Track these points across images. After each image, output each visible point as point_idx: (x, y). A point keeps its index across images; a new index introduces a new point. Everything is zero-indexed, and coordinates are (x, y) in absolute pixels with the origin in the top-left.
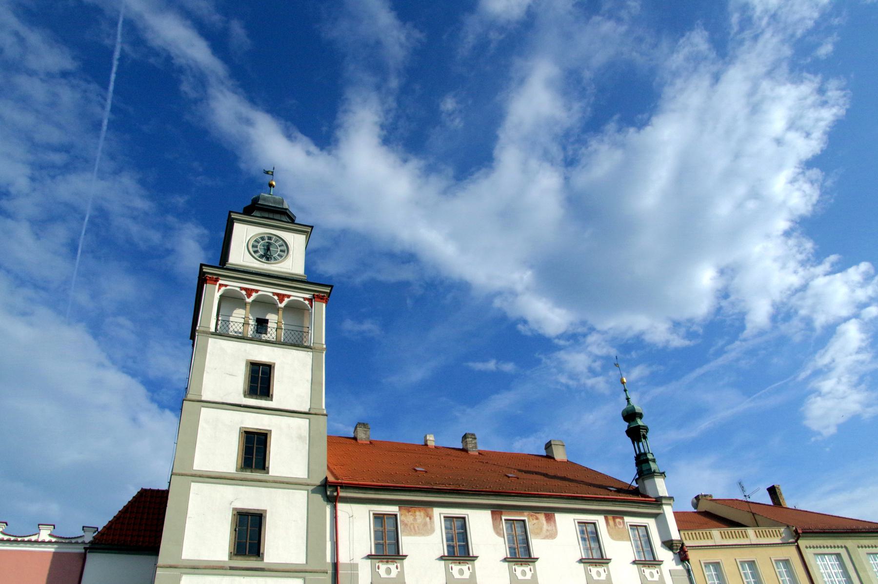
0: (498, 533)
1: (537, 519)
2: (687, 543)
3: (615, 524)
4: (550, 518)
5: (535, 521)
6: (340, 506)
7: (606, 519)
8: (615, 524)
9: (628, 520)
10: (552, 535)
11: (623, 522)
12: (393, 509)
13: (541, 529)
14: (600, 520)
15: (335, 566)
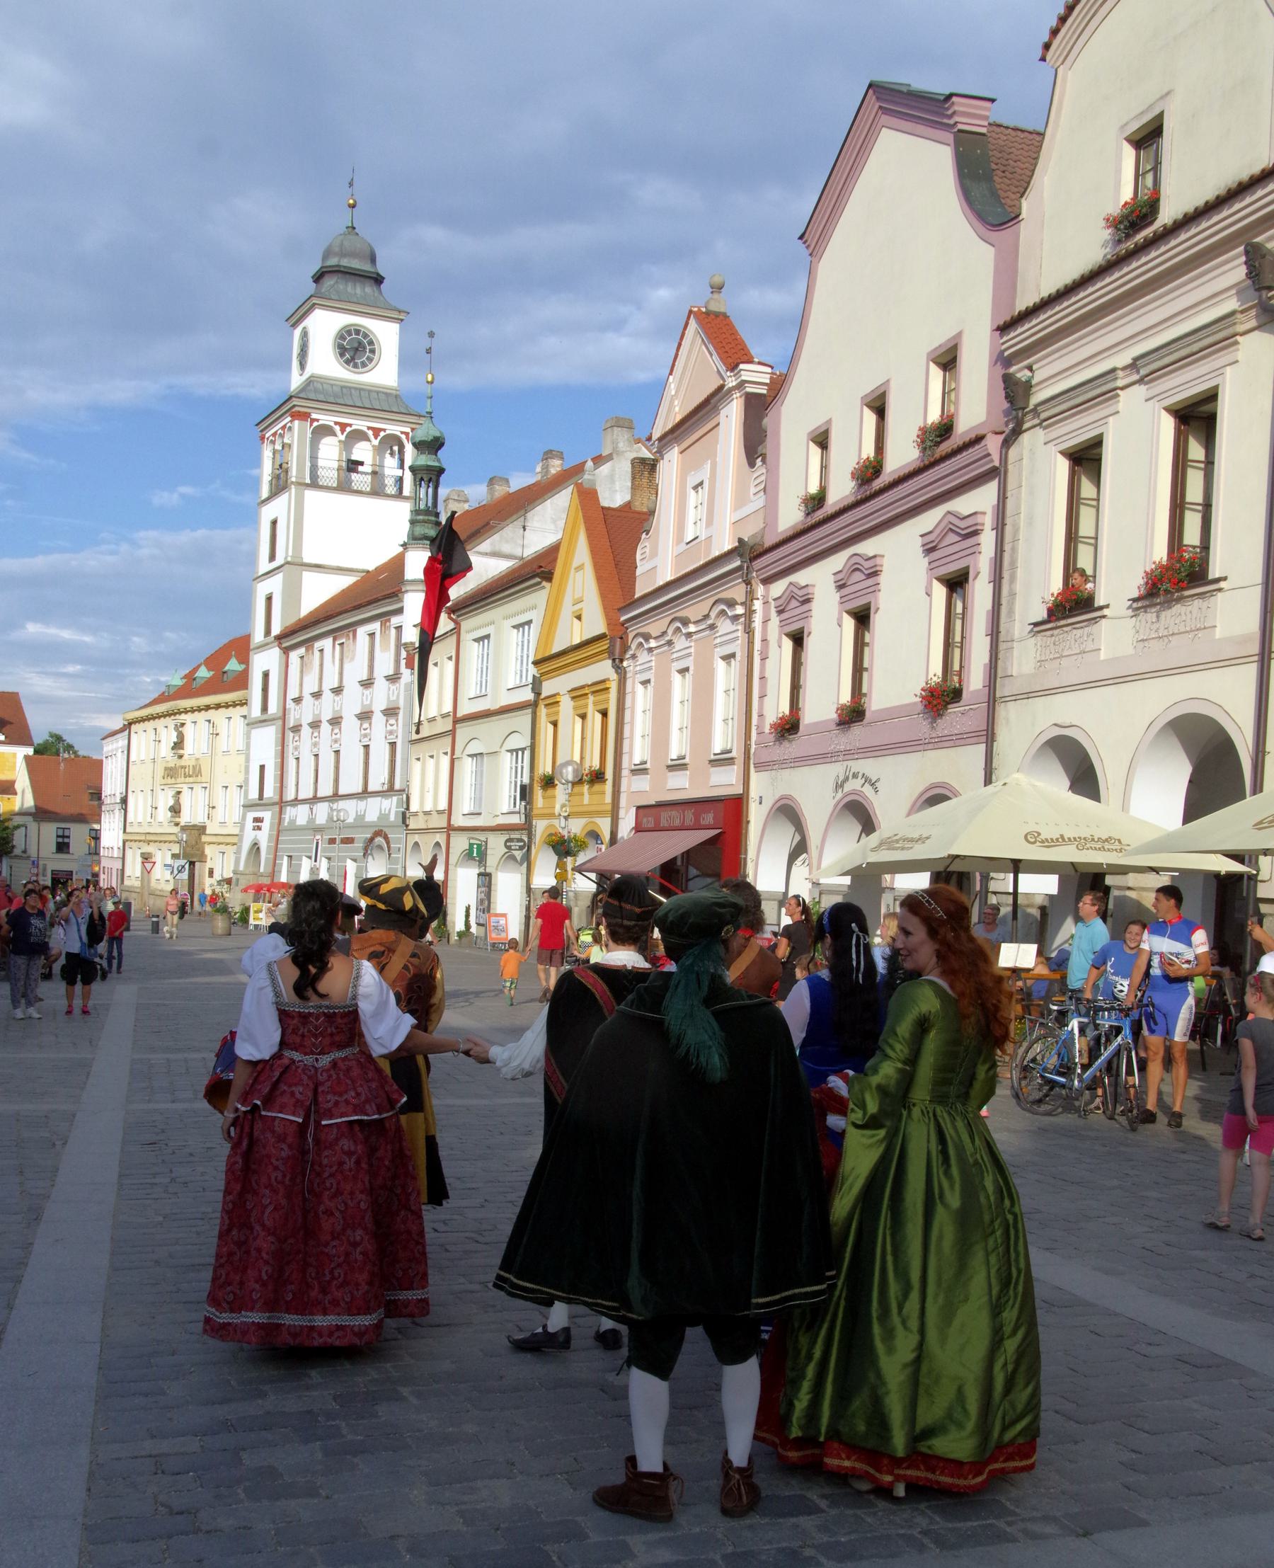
9: (395, 620)
10: (352, 659)
12: (302, 651)
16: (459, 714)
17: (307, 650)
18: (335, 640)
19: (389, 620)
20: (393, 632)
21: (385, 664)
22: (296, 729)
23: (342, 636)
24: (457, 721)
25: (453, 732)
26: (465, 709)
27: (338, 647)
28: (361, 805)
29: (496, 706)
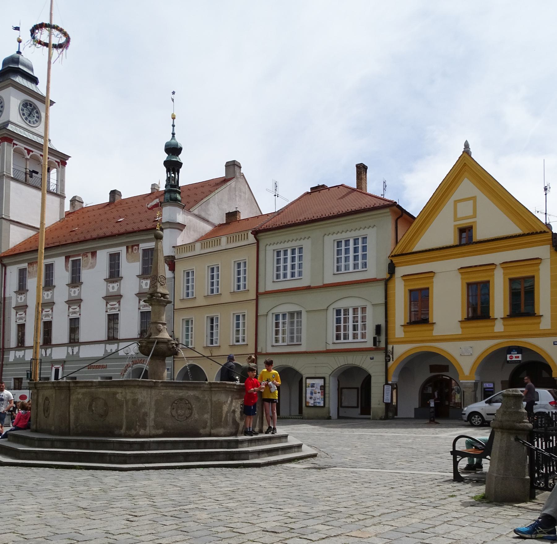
0: (67, 270)
1: (87, 257)
2: (176, 257)
3: (132, 251)
4: (94, 254)
5: (86, 258)
6: (9, 269)
7: (127, 248)
8: (132, 251)
9: (143, 246)
10: (93, 266)
11: (138, 248)
12: (25, 265)
13: (88, 263)
14: (124, 249)
15: (4, 298)
16: (261, 290)
17: (30, 264)
18: (67, 258)
19: (138, 245)
20: (141, 252)
21: (130, 268)
22: (23, 307)
23: (79, 255)
24: (258, 294)
25: (257, 299)
26: (270, 287)
27: (70, 262)
28: (112, 347)
29: (320, 284)
